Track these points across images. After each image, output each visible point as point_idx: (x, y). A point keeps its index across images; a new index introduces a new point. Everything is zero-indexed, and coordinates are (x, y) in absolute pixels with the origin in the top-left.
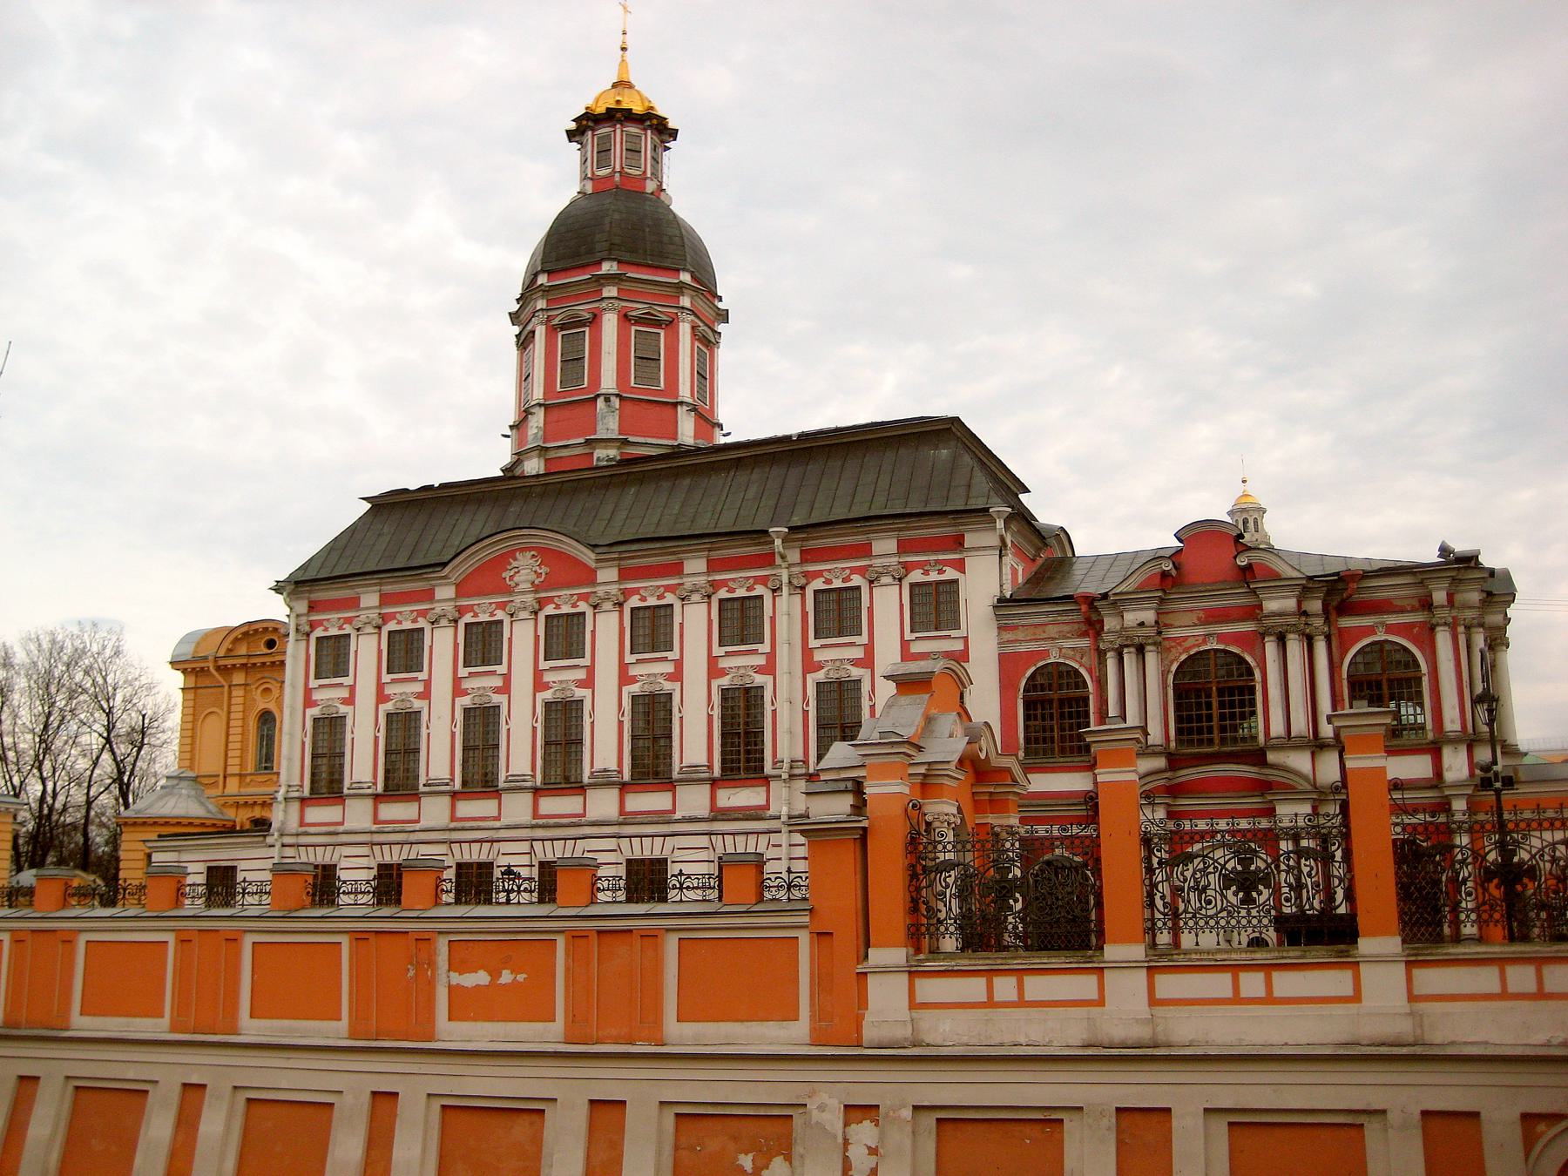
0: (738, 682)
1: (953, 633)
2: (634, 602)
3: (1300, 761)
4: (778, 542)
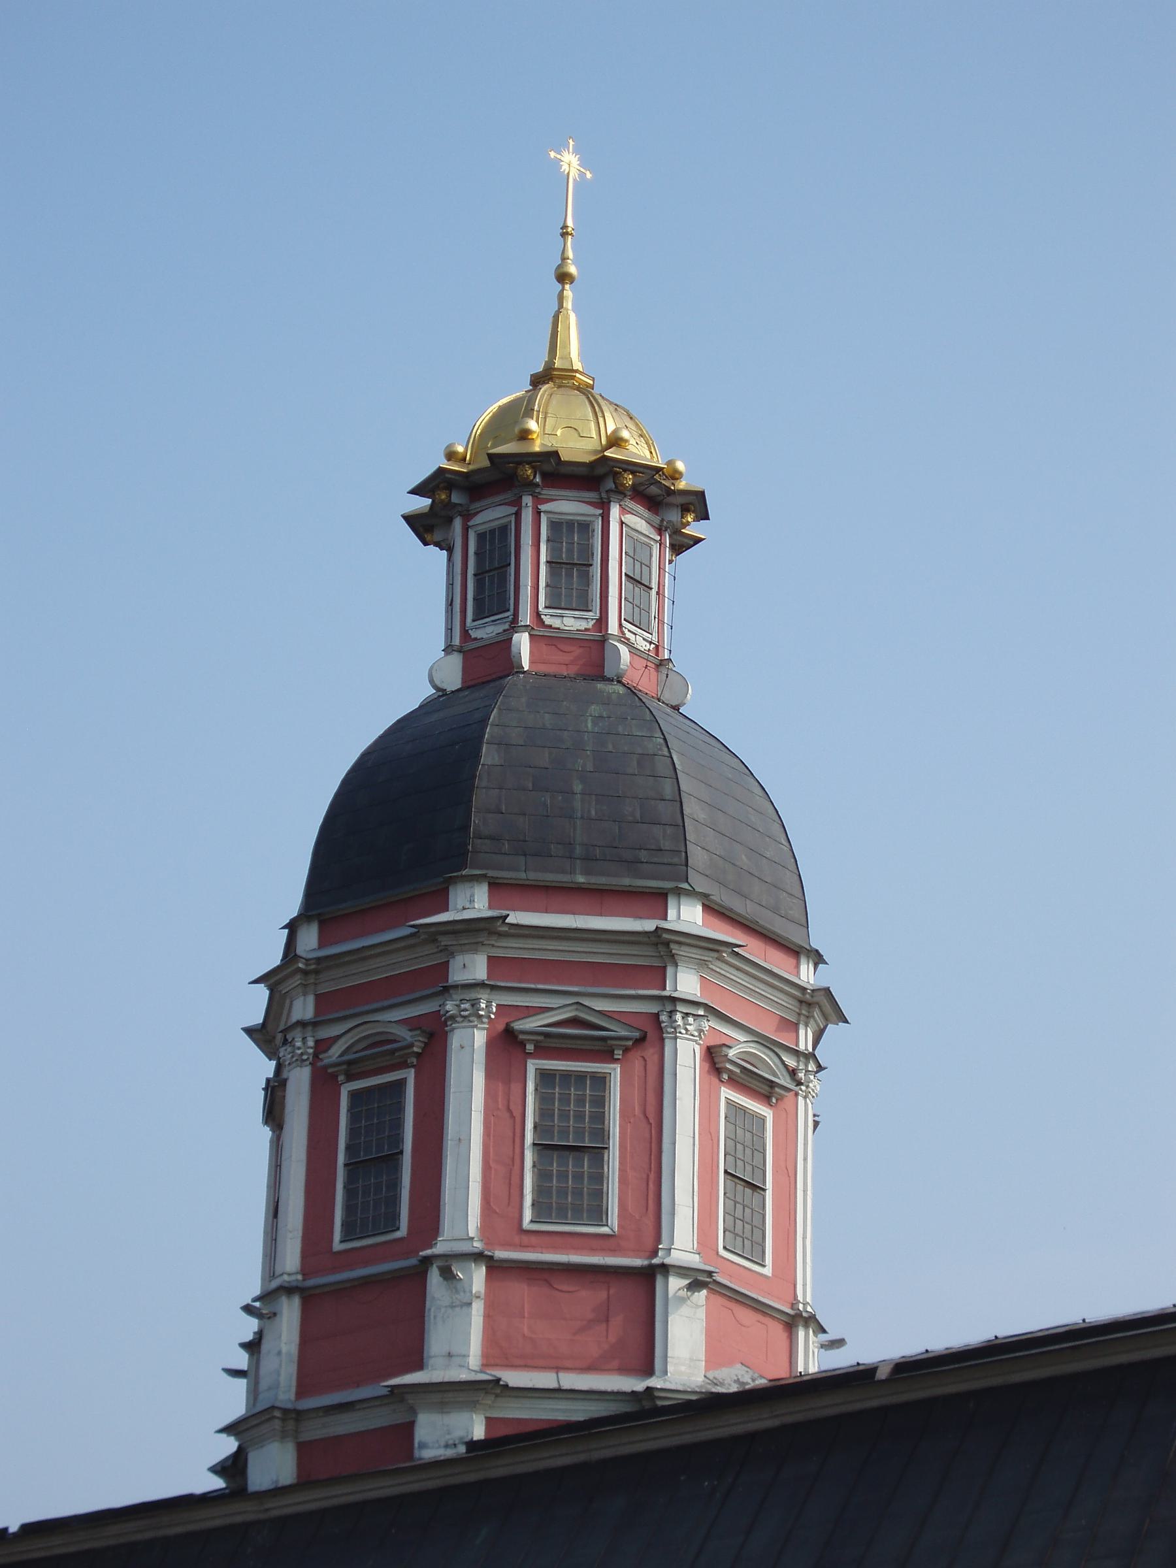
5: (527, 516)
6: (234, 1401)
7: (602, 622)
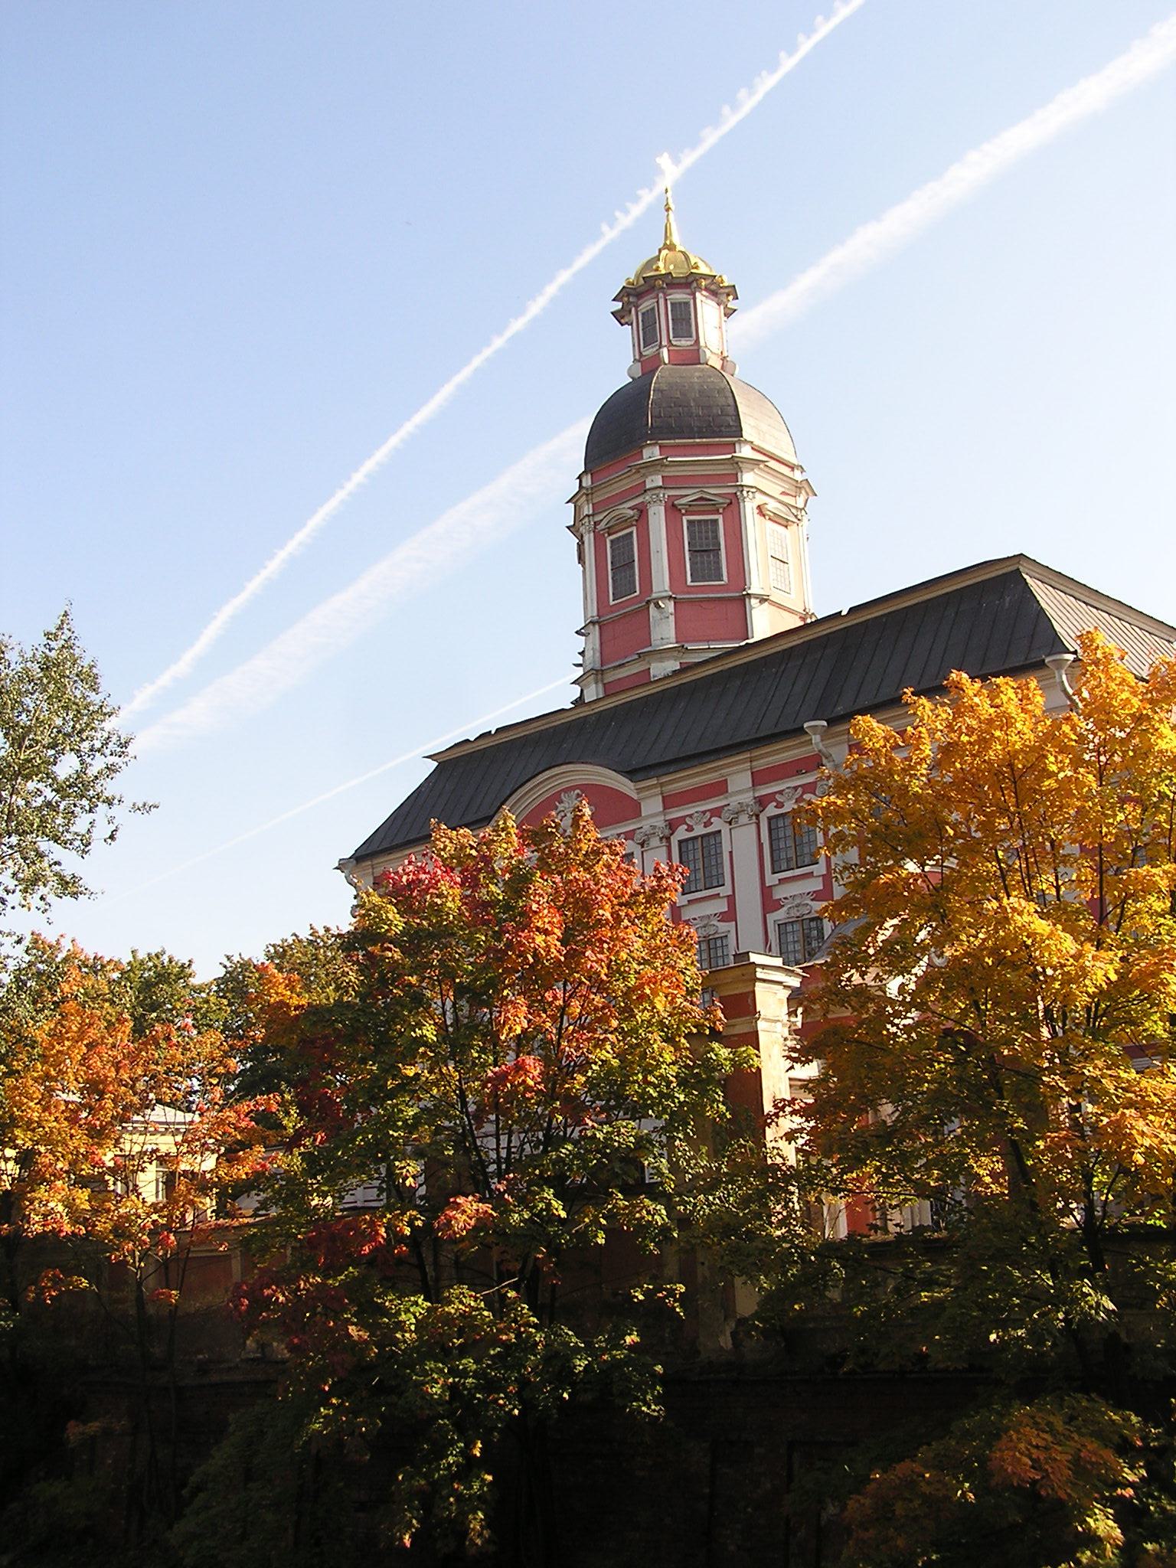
0: (794, 913)
2: (681, 833)
5: (661, 302)
7: (697, 341)
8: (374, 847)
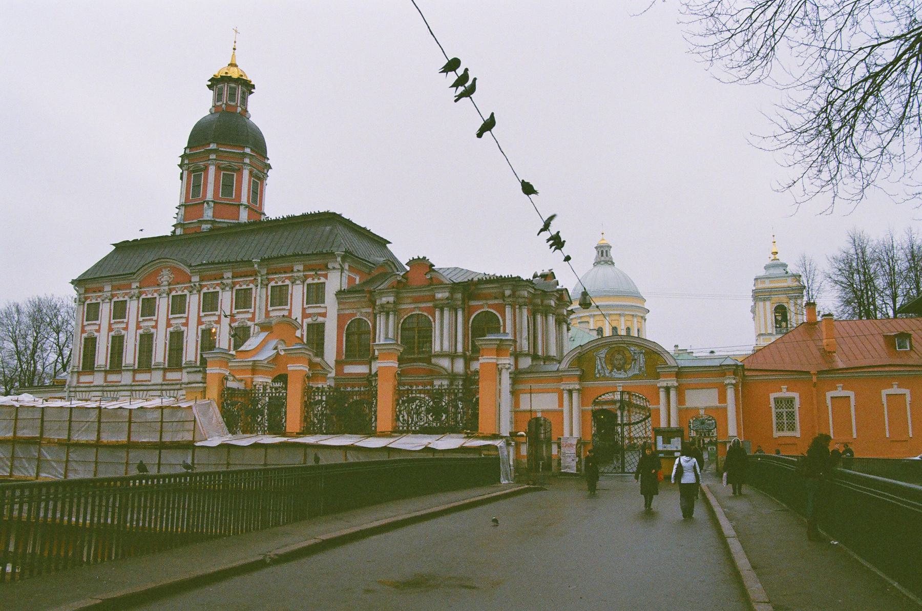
1: (322, 305)
3: (445, 363)
4: (256, 266)
6: (175, 222)
8: (86, 277)
